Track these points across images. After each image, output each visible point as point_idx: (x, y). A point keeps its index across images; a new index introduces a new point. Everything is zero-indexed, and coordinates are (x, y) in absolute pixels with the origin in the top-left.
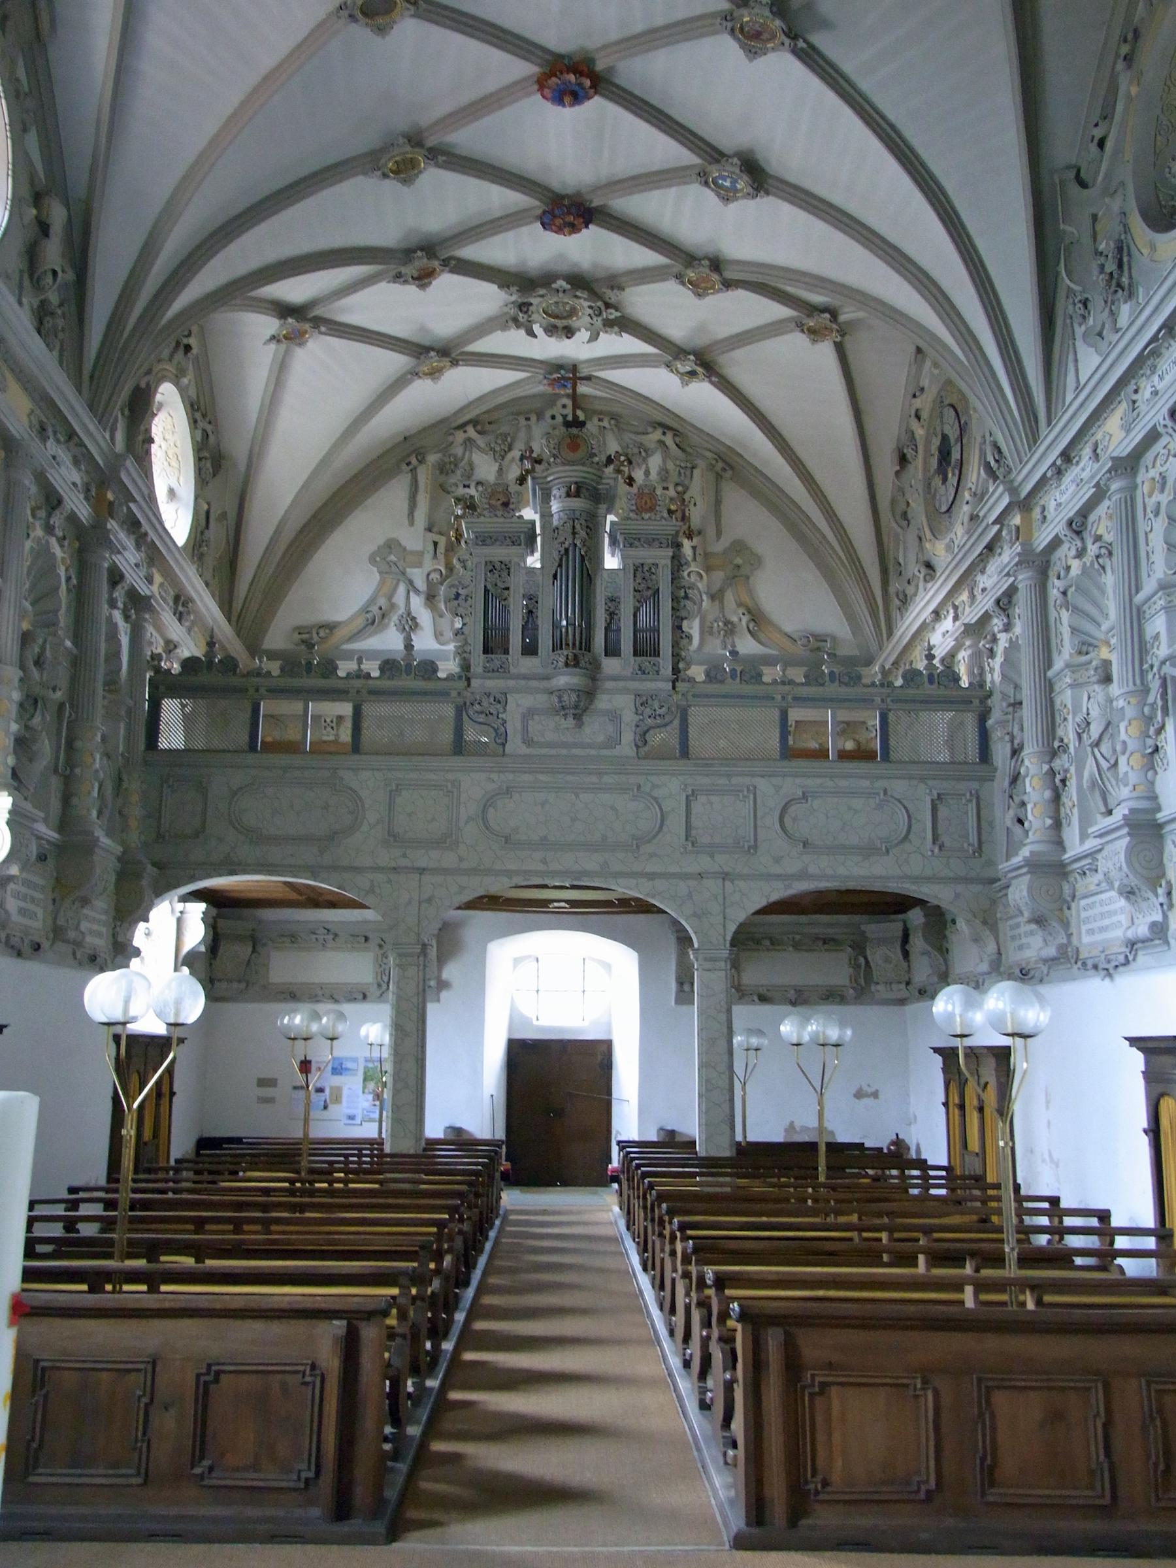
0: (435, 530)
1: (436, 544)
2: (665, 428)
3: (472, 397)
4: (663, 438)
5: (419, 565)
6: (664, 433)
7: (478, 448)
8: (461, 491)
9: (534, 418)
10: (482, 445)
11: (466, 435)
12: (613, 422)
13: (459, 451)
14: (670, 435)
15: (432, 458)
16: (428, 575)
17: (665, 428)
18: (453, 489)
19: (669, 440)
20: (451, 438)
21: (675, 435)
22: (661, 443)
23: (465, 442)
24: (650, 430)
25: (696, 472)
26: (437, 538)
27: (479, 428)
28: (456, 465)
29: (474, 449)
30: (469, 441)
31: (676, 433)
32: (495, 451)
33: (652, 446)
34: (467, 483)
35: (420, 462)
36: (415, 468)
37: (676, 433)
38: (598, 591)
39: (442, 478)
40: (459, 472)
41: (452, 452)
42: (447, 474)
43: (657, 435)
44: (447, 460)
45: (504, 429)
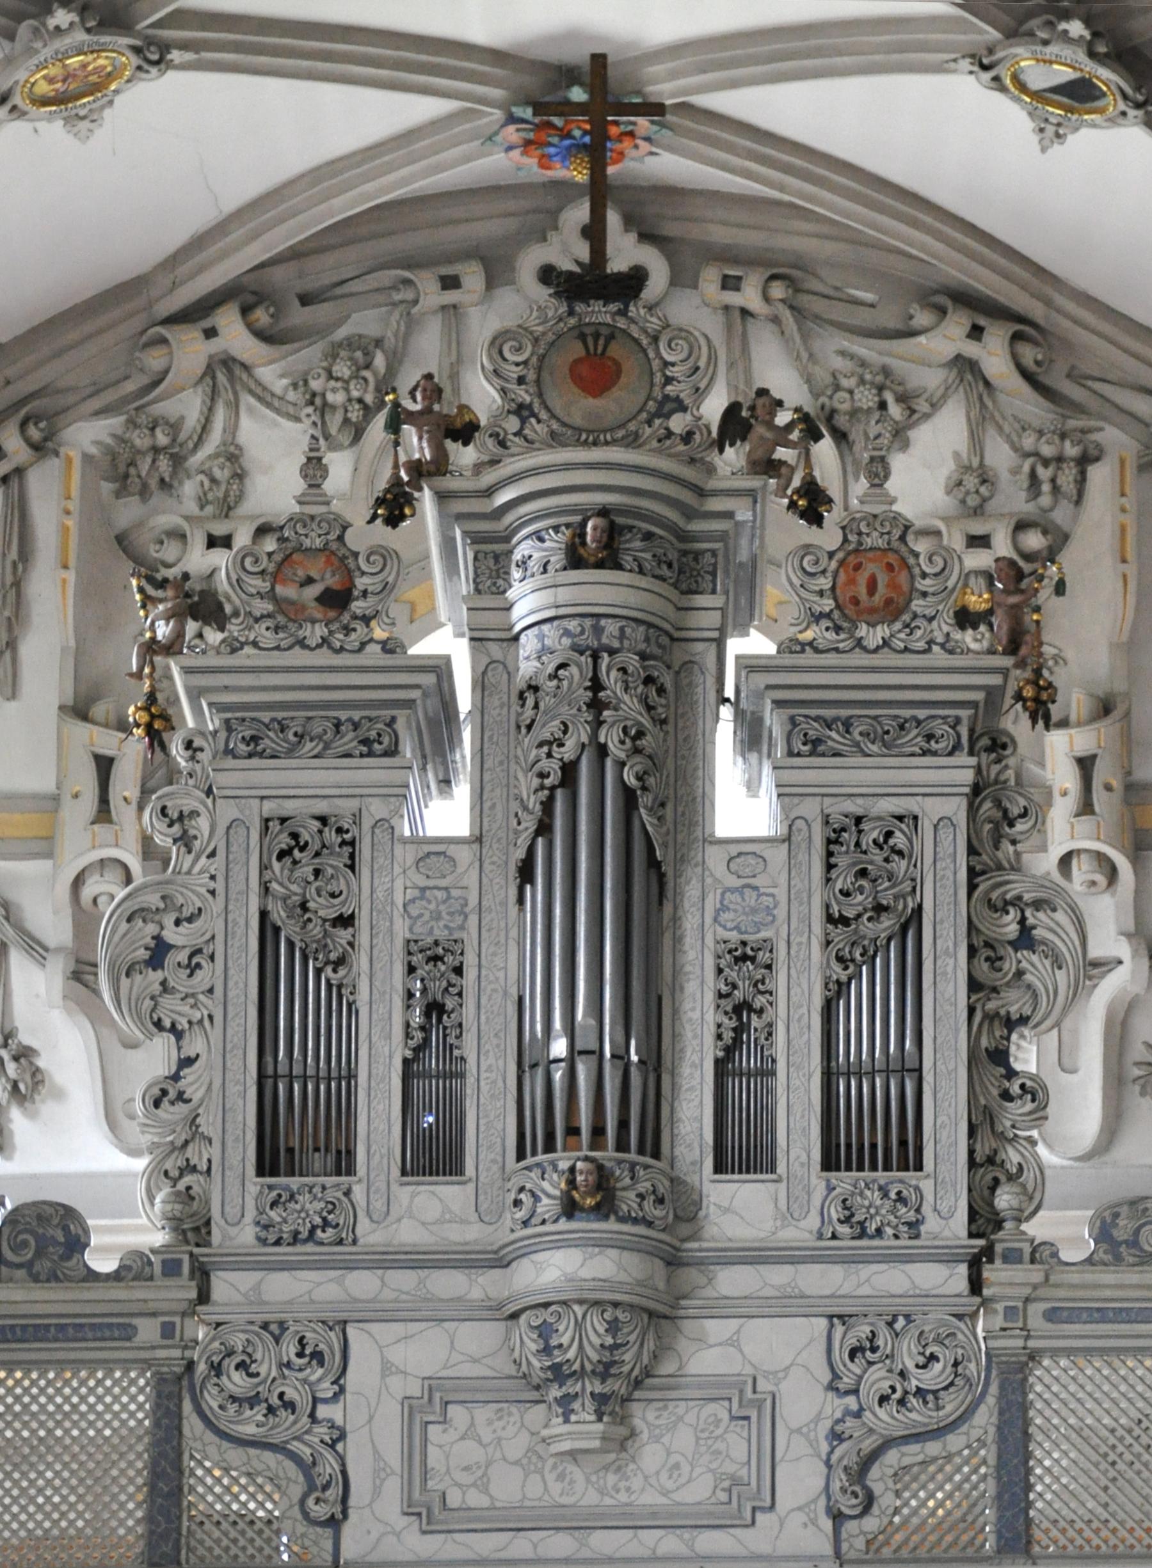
0: (99, 710)
1: (104, 765)
2: (982, 310)
3: (233, 199)
4: (971, 349)
5: (45, 846)
6: (976, 332)
7: (265, 397)
8: (199, 560)
9: (473, 277)
10: (279, 385)
11: (215, 346)
12: (778, 291)
13: (188, 406)
14: (997, 339)
15: (87, 435)
16: (78, 882)
17: (982, 310)
18: (170, 551)
19: (994, 355)
20: (154, 360)
21: (1017, 337)
22: (966, 368)
23: (209, 371)
24: (923, 318)
25: (1100, 475)
26: (107, 741)
27: (261, 316)
28: (178, 461)
29: (247, 400)
30: (225, 371)
31: (1023, 329)
32: (325, 408)
33: (931, 379)
34: (219, 529)
35: (40, 449)
36: (19, 471)
37: (1023, 329)
38: (690, 923)
39: (128, 512)
40: (189, 488)
41: (159, 409)
42: (144, 493)
43: (947, 339)
44: (140, 440)
45: (365, 322)
